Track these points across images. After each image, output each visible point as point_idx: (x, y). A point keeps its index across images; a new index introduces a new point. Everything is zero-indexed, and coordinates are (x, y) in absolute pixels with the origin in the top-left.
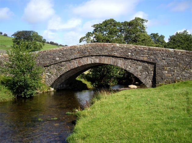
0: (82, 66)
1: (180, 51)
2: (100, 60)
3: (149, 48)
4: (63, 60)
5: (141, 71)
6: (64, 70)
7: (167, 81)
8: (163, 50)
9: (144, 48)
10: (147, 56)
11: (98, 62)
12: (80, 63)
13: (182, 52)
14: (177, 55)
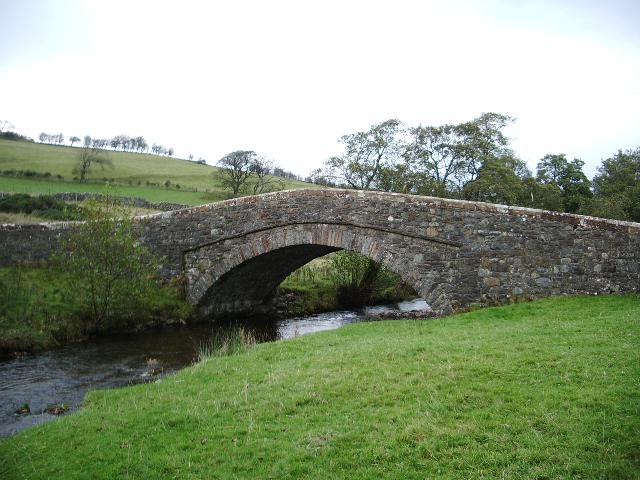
0: (272, 252)
1: (526, 212)
2: (316, 236)
3: (442, 202)
4: (226, 234)
5: (423, 268)
6: (231, 260)
7: (488, 297)
8: (479, 209)
9: (428, 202)
10: (437, 224)
11: (311, 242)
12: (266, 243)
13: (530, 215)
14: (518, 223)
